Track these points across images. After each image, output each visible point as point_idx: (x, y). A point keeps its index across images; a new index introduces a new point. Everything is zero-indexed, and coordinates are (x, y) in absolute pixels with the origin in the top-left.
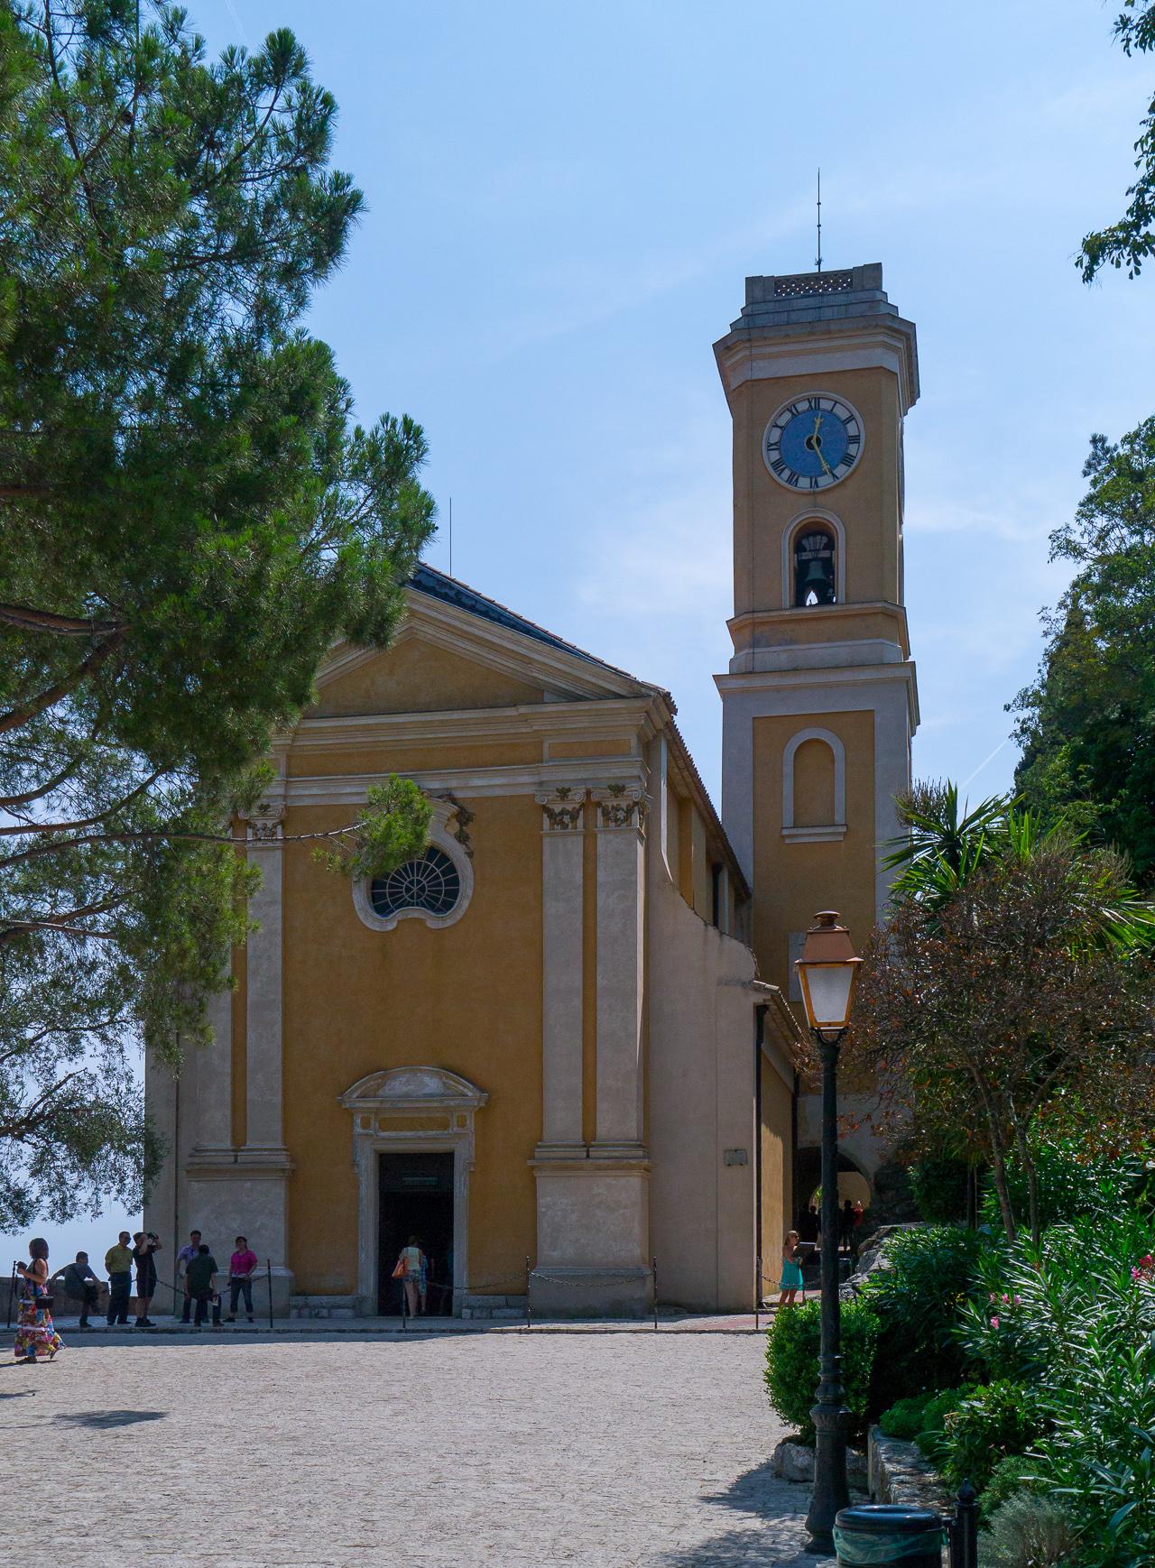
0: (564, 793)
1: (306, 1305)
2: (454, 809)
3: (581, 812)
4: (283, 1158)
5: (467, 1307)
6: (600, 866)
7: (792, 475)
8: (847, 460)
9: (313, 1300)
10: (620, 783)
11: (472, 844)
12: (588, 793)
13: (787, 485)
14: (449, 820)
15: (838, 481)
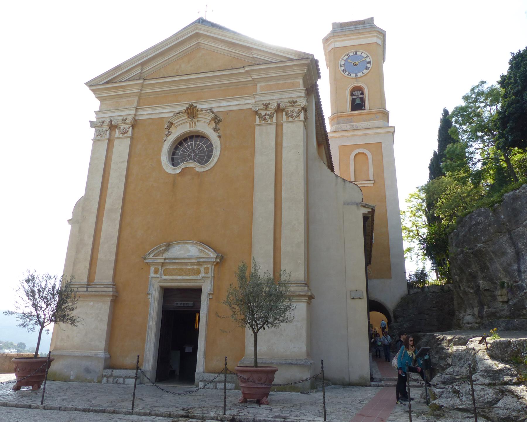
0: (266, 106)
1: (111, 376)
2: (212, 116)
3: (275, 114)
4: (111, 289)
5: (201, 381)
6: (284, 138)
7: (349, 73)
8: (367, 68)
9: (116, 372)
10: (295, 100)
11: (221, 133)
12: (278, 105)
13: (347, 76)
14: (210, 121)
15: (364, 74)
